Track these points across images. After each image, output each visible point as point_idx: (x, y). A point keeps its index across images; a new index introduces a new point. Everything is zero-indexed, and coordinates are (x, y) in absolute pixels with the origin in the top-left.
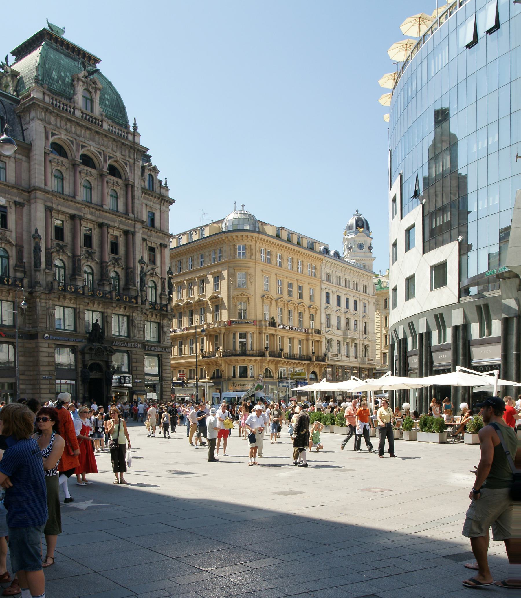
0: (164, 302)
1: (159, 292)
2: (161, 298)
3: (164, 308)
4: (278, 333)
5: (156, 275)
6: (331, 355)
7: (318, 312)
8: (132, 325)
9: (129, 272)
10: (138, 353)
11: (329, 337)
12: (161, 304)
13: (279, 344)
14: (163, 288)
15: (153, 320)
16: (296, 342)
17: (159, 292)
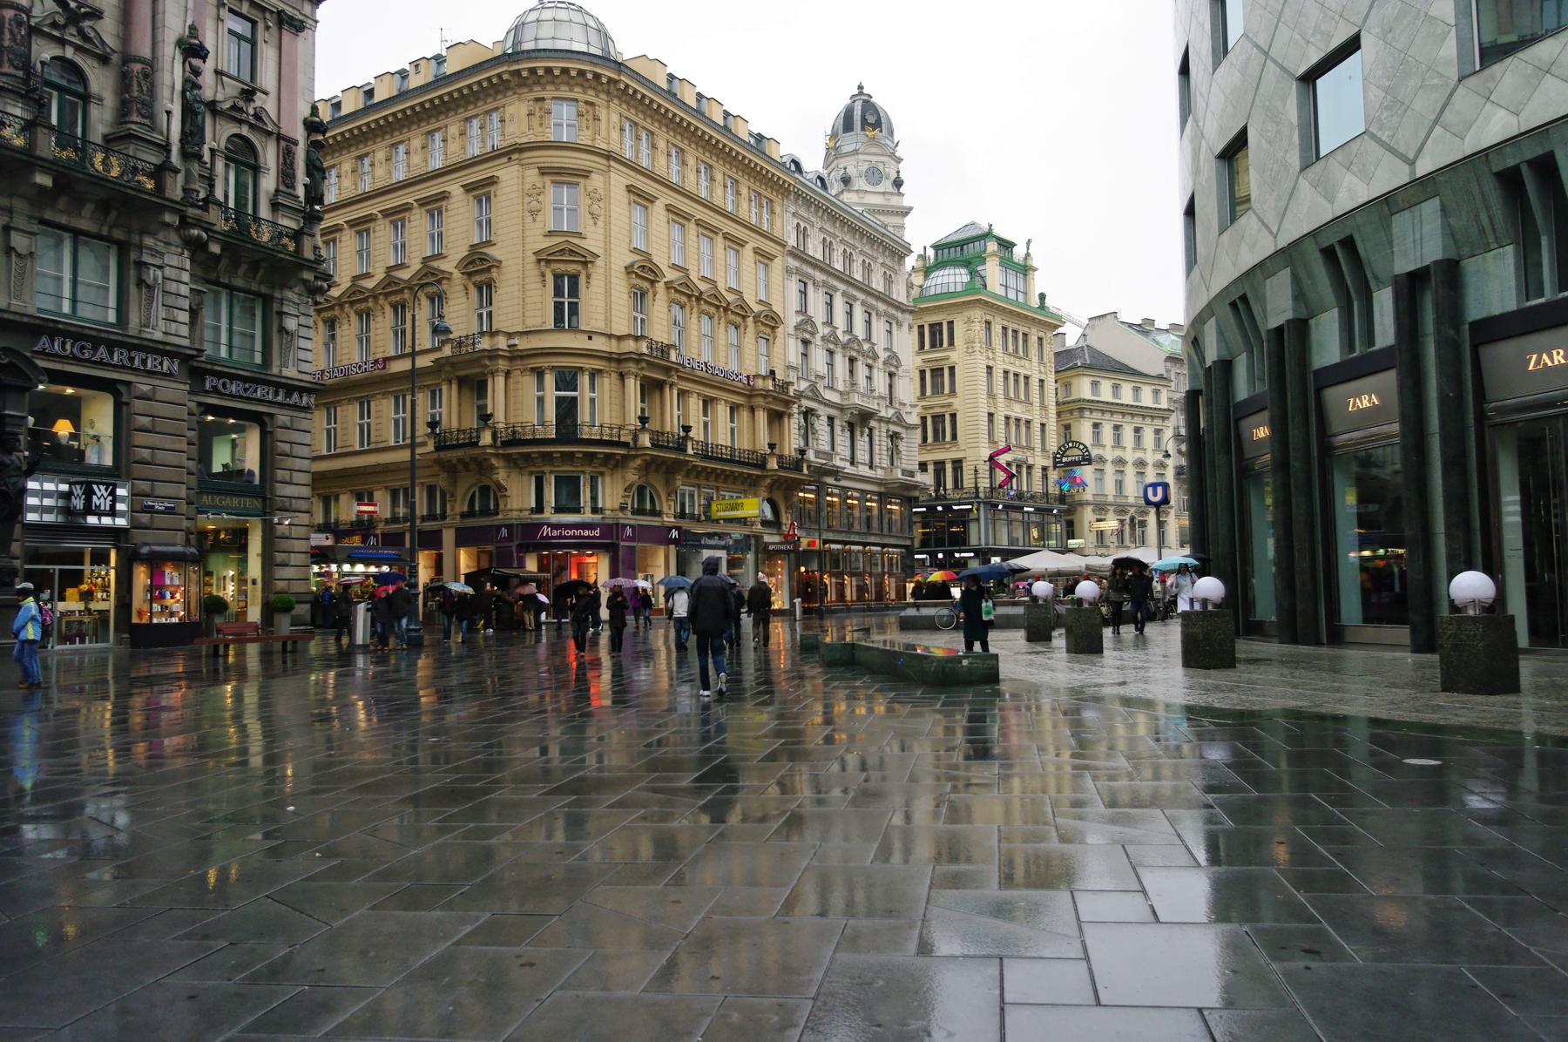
0: (288, 223)
1: (268, 183)
2: (275, 206)
3: (285, 240)
4: (675, 379)
5: (257, 116)
6: (818, 453)
7: (780, 331)
8: (141, 282)
9: (137, 84)
10: (163, 394)
11: (805, 403)
12: (275, 224)
13: (676, 412)
14: (287, 176)
15: (238, 282)
16: (722, 411)
17: (268, 183)
